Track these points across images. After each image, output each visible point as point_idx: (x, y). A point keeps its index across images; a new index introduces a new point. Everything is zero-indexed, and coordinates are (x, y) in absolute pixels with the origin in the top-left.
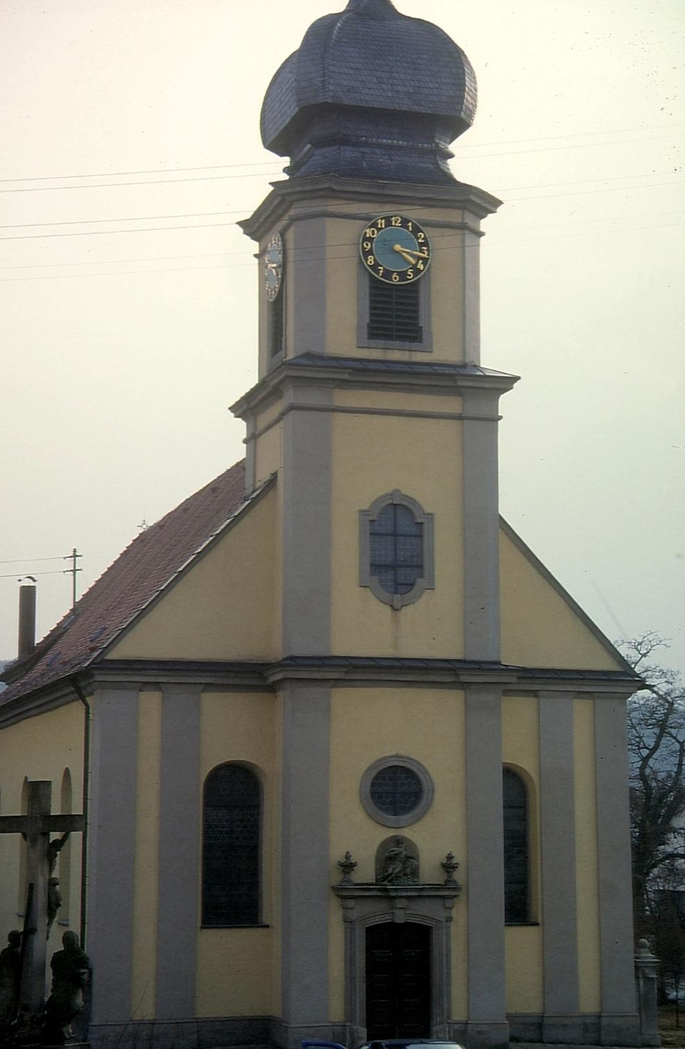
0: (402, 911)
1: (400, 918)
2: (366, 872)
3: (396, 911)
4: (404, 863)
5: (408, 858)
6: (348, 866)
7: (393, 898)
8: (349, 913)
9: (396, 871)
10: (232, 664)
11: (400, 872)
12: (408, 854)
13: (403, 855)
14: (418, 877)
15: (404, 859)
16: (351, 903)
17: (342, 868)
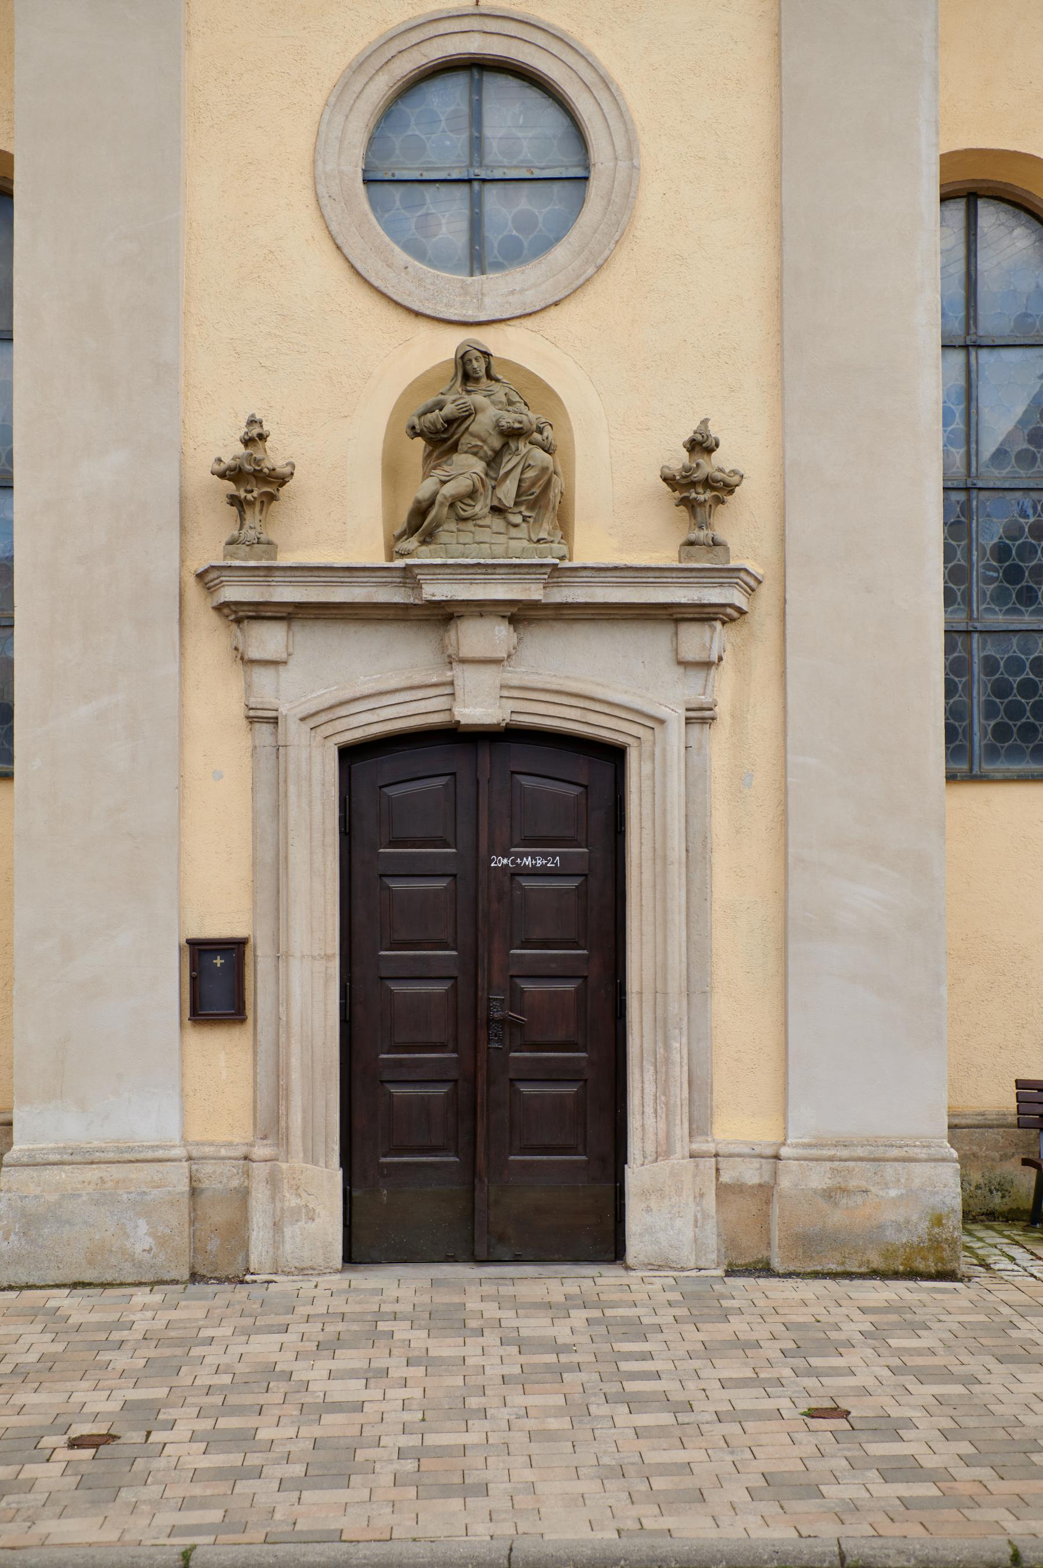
0: (489, 676)
1: (479, 706)
2: (342, 517)
3: (467, 678)
4: (493, 461)
5: (512, 435)
6: (254, 483)
7: (444, 615)
8: (263, 678)
9: (448, 490)
10: (503, 73)
11: (472, 494)
12: (509, 419)
13: (483, 423)
14: (564, 523)
15: (496, 443)
16: (268, 639)
17: (229, 486)
